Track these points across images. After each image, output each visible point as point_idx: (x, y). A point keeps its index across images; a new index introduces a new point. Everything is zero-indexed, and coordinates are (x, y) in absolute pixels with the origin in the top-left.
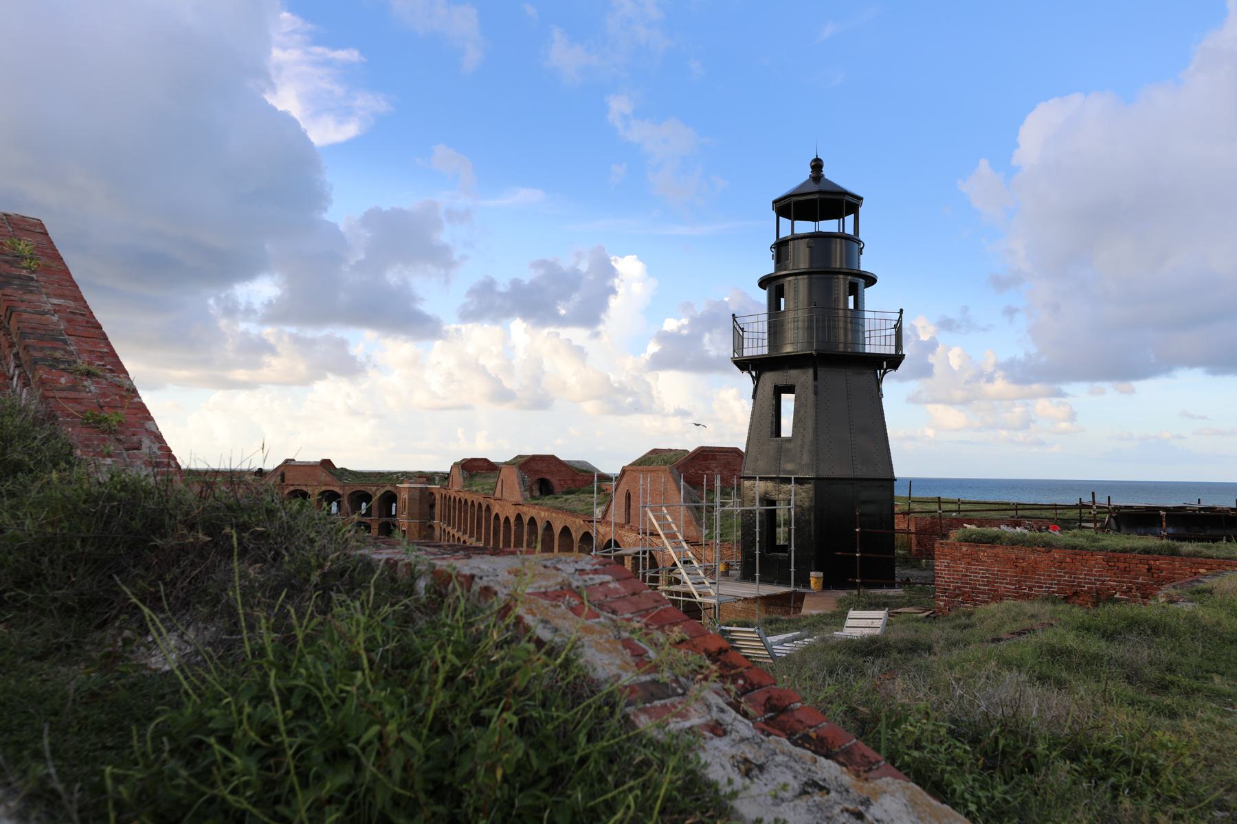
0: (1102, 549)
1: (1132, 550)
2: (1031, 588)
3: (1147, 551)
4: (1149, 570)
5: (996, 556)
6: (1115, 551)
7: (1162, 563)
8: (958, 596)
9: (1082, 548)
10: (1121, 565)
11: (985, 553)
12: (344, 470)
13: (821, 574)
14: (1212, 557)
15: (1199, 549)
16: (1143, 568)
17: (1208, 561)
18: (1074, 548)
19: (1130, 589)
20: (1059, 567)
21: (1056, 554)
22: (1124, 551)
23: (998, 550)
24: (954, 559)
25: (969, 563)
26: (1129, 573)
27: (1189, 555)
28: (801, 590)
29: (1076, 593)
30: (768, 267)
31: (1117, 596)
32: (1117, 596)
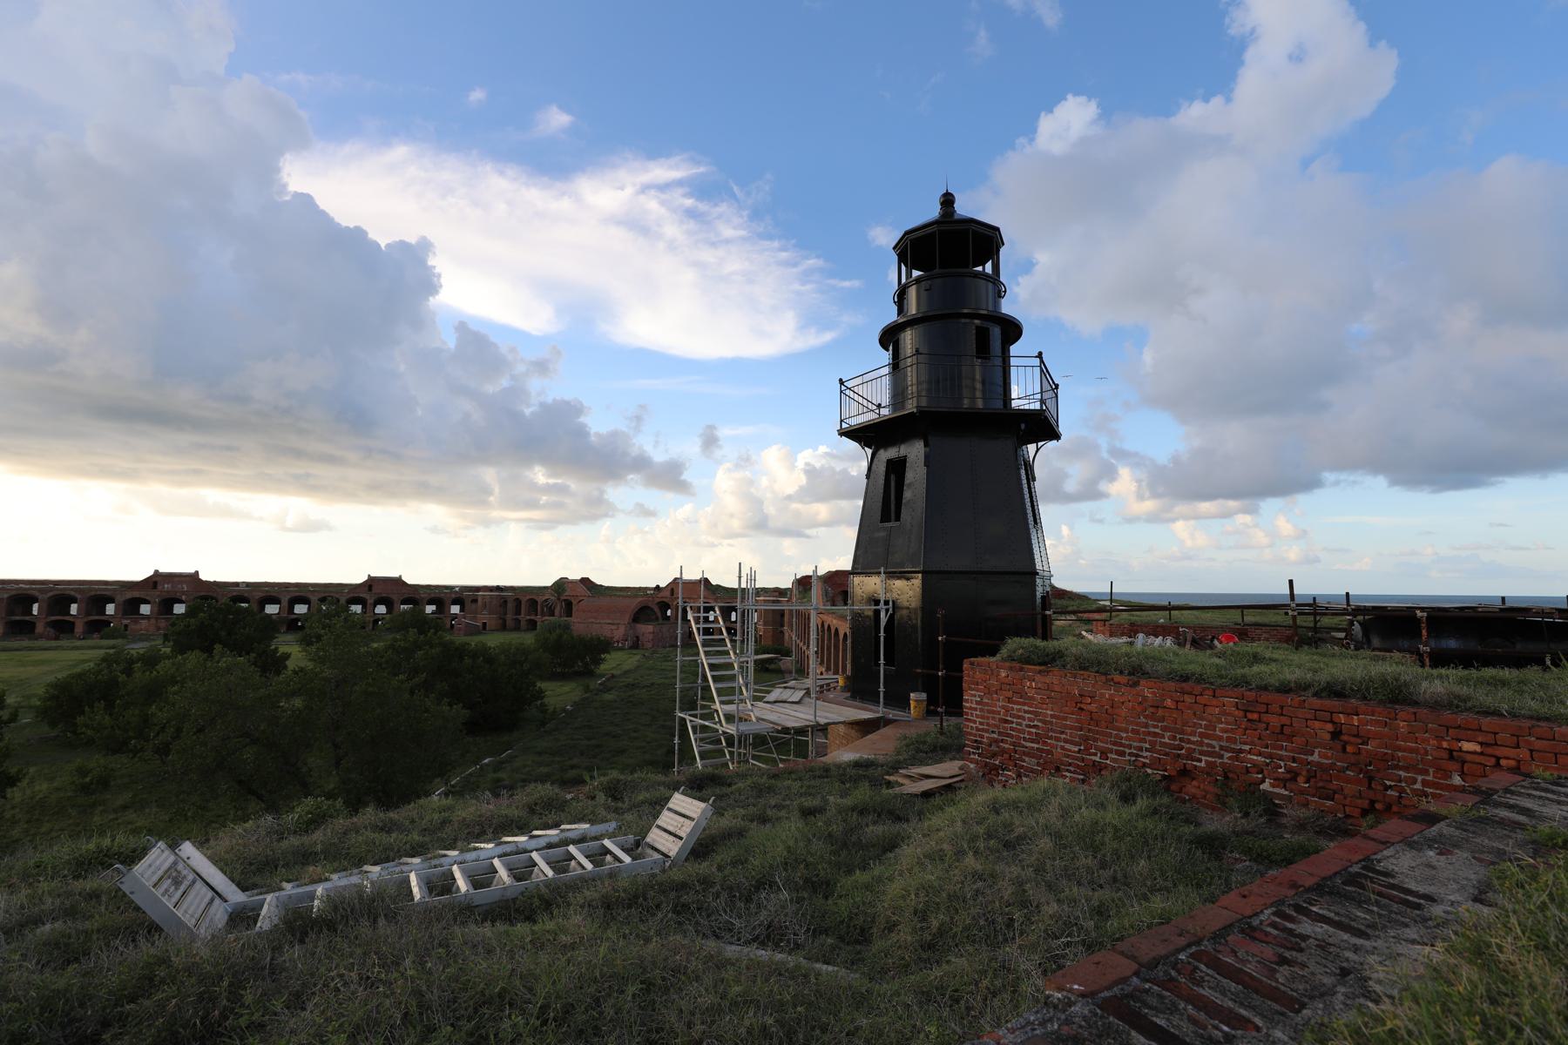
0: (1242, 682)
1: (1302, 687)
2: (1104, 754)
3: (1335, 691)
4: (1336, 735)
5: (1049, 688)
6: (1265, 688)
7: (1365, 720)
8: (994, 755)
9: (1200, 679)
10: (1275, 721)
11: (1033, 683)
12: (718, 586)
13: (924, 696)
14: (1497, 713)
15: (1465, 691)
16: (1324, 730)
17: (1486, 722)
18: (1185, 678)
19: (1293, 775)
20: (1152, 717)
21: (1147, 690)
22: (1285, 689)
23: (1054, 678)
24: (988, 691)
25: (1009, 700)
26: (1290, 738)
27: (1436, 705)
28: (892, 714)
29: (1185, 772)
30: (891, 315)
31: (1266, 786)
32: (1266, 786)
